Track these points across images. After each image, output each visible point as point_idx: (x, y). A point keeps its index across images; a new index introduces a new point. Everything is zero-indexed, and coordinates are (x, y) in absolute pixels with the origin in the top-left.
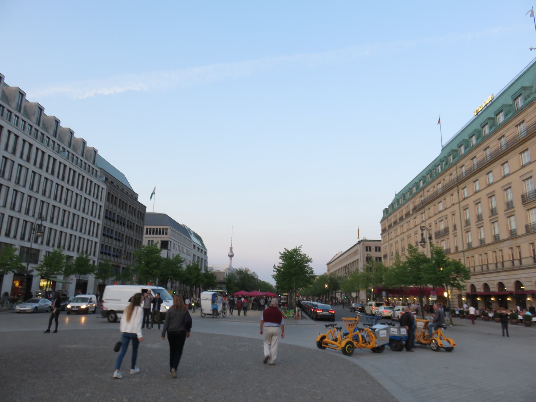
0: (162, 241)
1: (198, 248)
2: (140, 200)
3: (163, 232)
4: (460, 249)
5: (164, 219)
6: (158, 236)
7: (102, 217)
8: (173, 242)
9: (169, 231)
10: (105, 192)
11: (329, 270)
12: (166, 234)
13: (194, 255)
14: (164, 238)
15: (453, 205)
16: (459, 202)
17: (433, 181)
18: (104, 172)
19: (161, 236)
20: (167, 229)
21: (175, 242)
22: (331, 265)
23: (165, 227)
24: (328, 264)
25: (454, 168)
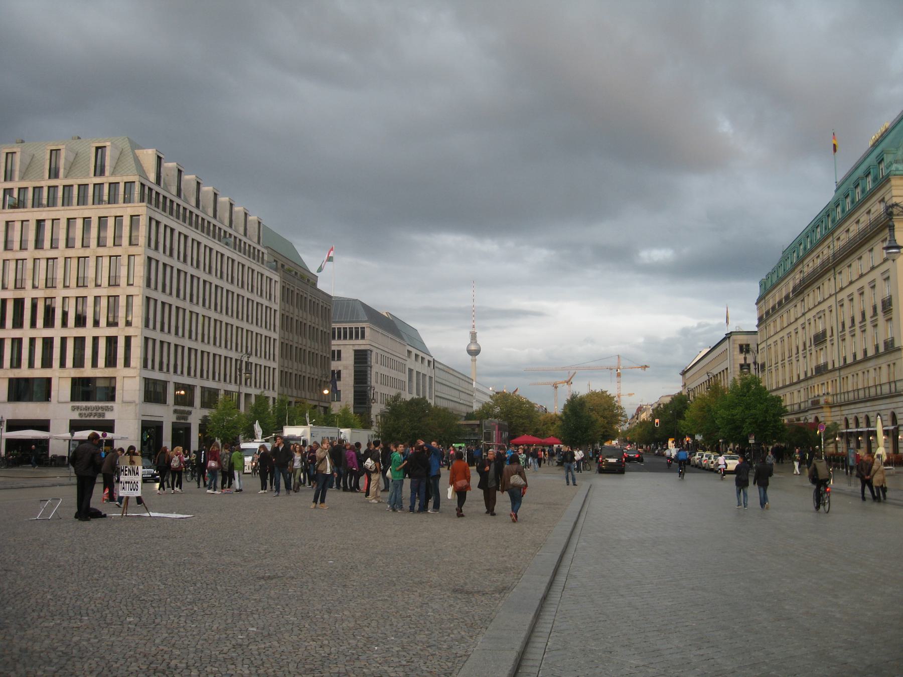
0: (356, 351)
1: (417, 356)
2: (320, 286)
3: (359, 334)
4: (837, 365)
5: (352, 307)
6: (348, 342)
7: (277, 329)
8: (375, 351)
9: (367, 332)
10: (278, 286)
11: (684, 386)
12: (363, 337)
13: (411, 370)
14: (360, 344)
15: (831, 296)
16: (836, 293)
17: (809, 254)
18: (272, 251)
19: (352, 342)
20: (363, 328)
21: (379, 351)
22: (688, 375)
23: (360, 325)
24: (684, 373)
25: (830, 239)
